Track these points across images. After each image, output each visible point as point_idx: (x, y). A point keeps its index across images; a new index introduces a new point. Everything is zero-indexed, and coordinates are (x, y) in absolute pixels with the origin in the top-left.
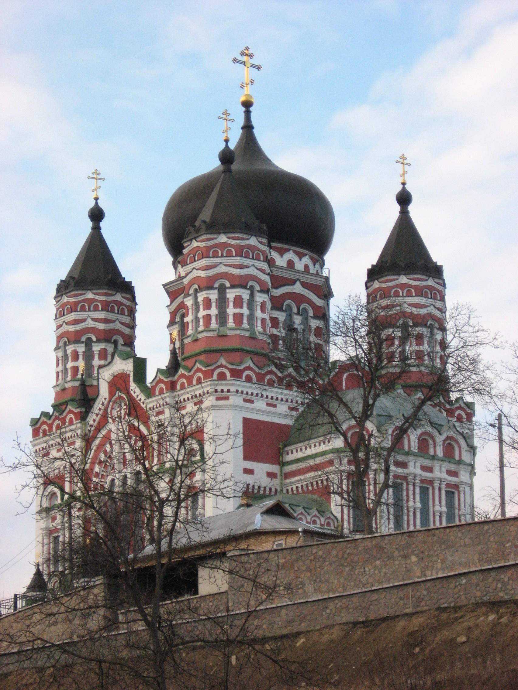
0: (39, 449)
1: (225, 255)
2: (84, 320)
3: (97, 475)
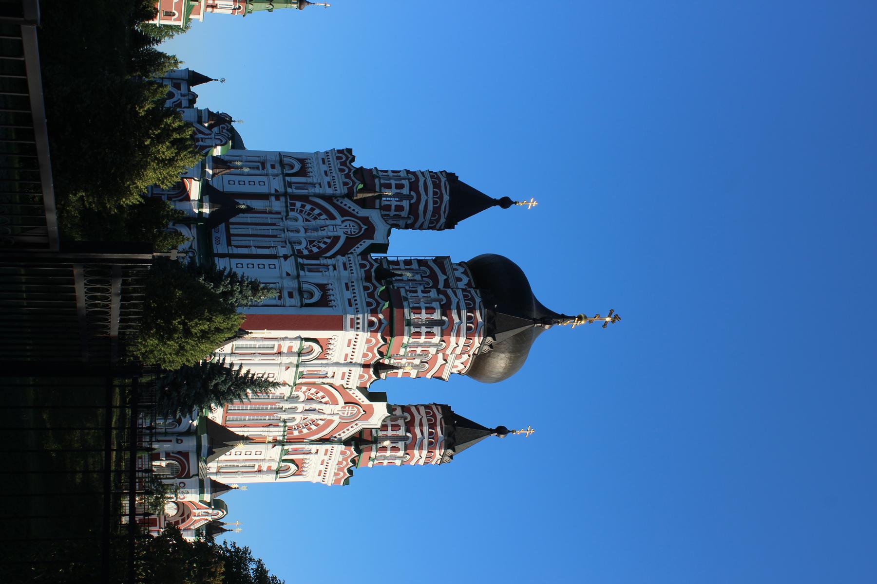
0: (329, 156)
1: (468, 325)
3: (303, 206)
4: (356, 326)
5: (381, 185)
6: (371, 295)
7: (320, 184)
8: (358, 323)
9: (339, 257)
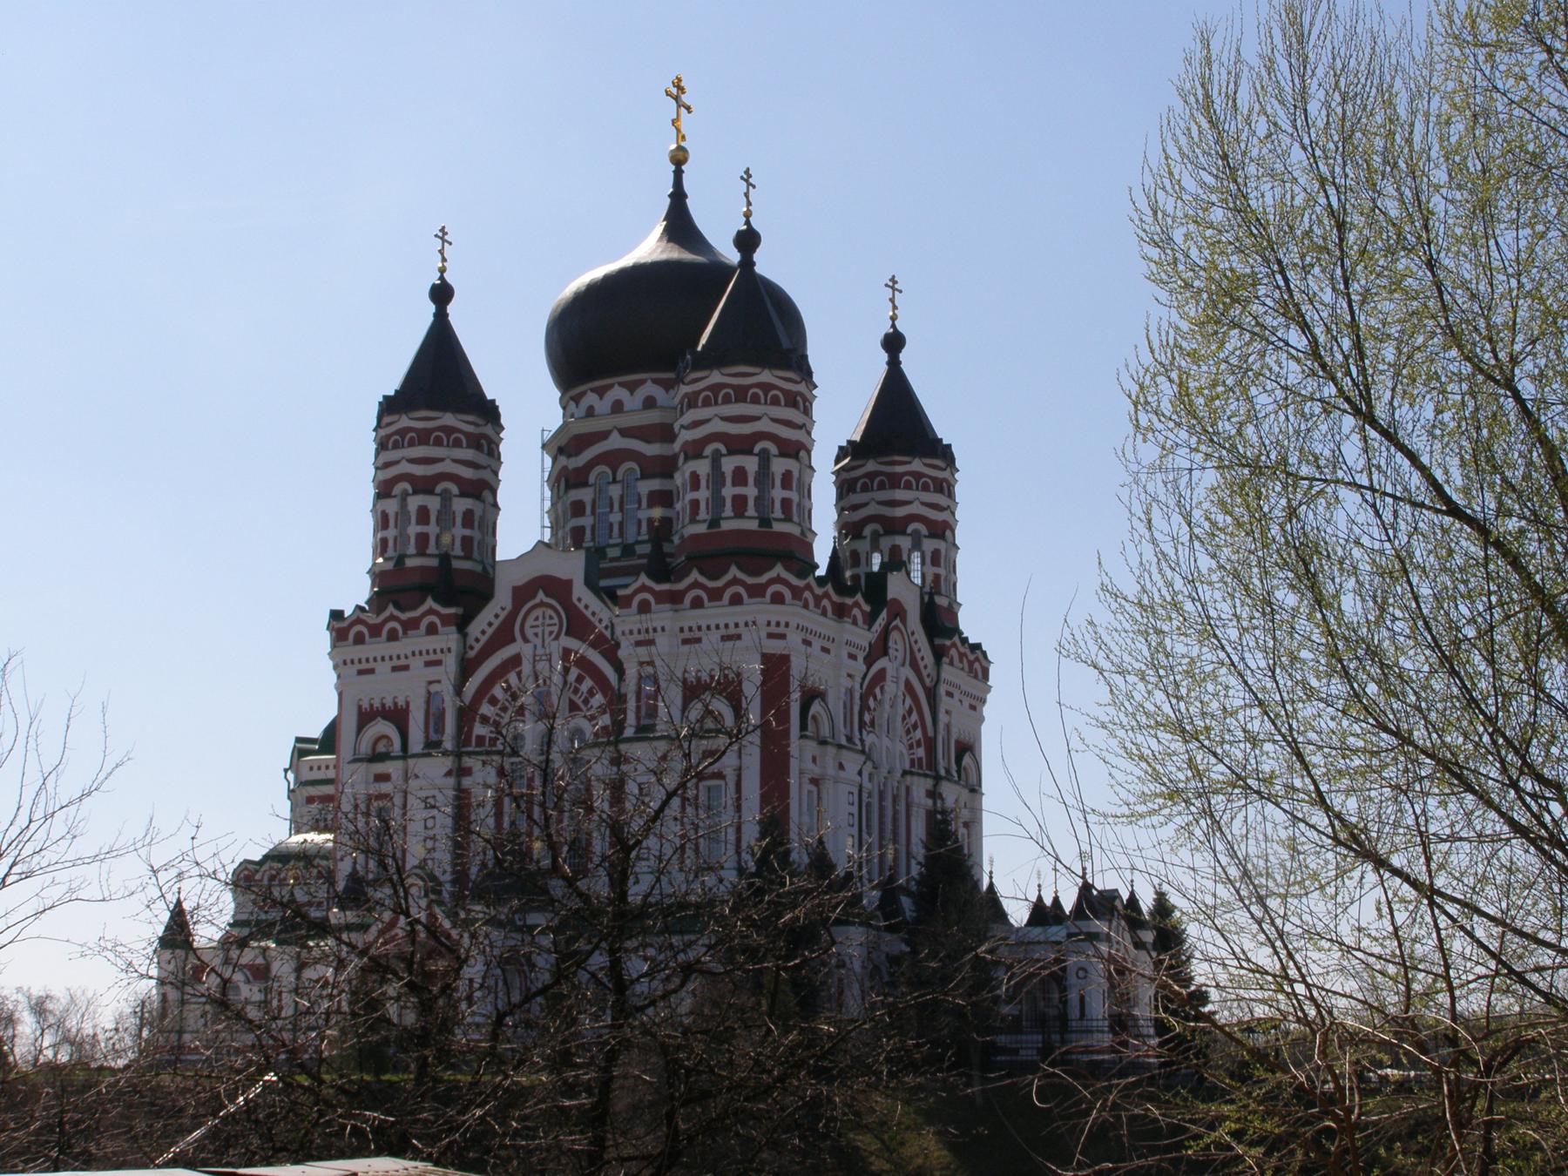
3: (485, 720)
4: (781, 630)
5: (421, 552)
6: (716, 595)
7: (430, 683)
8: (778, 624)
9: (622, 654)
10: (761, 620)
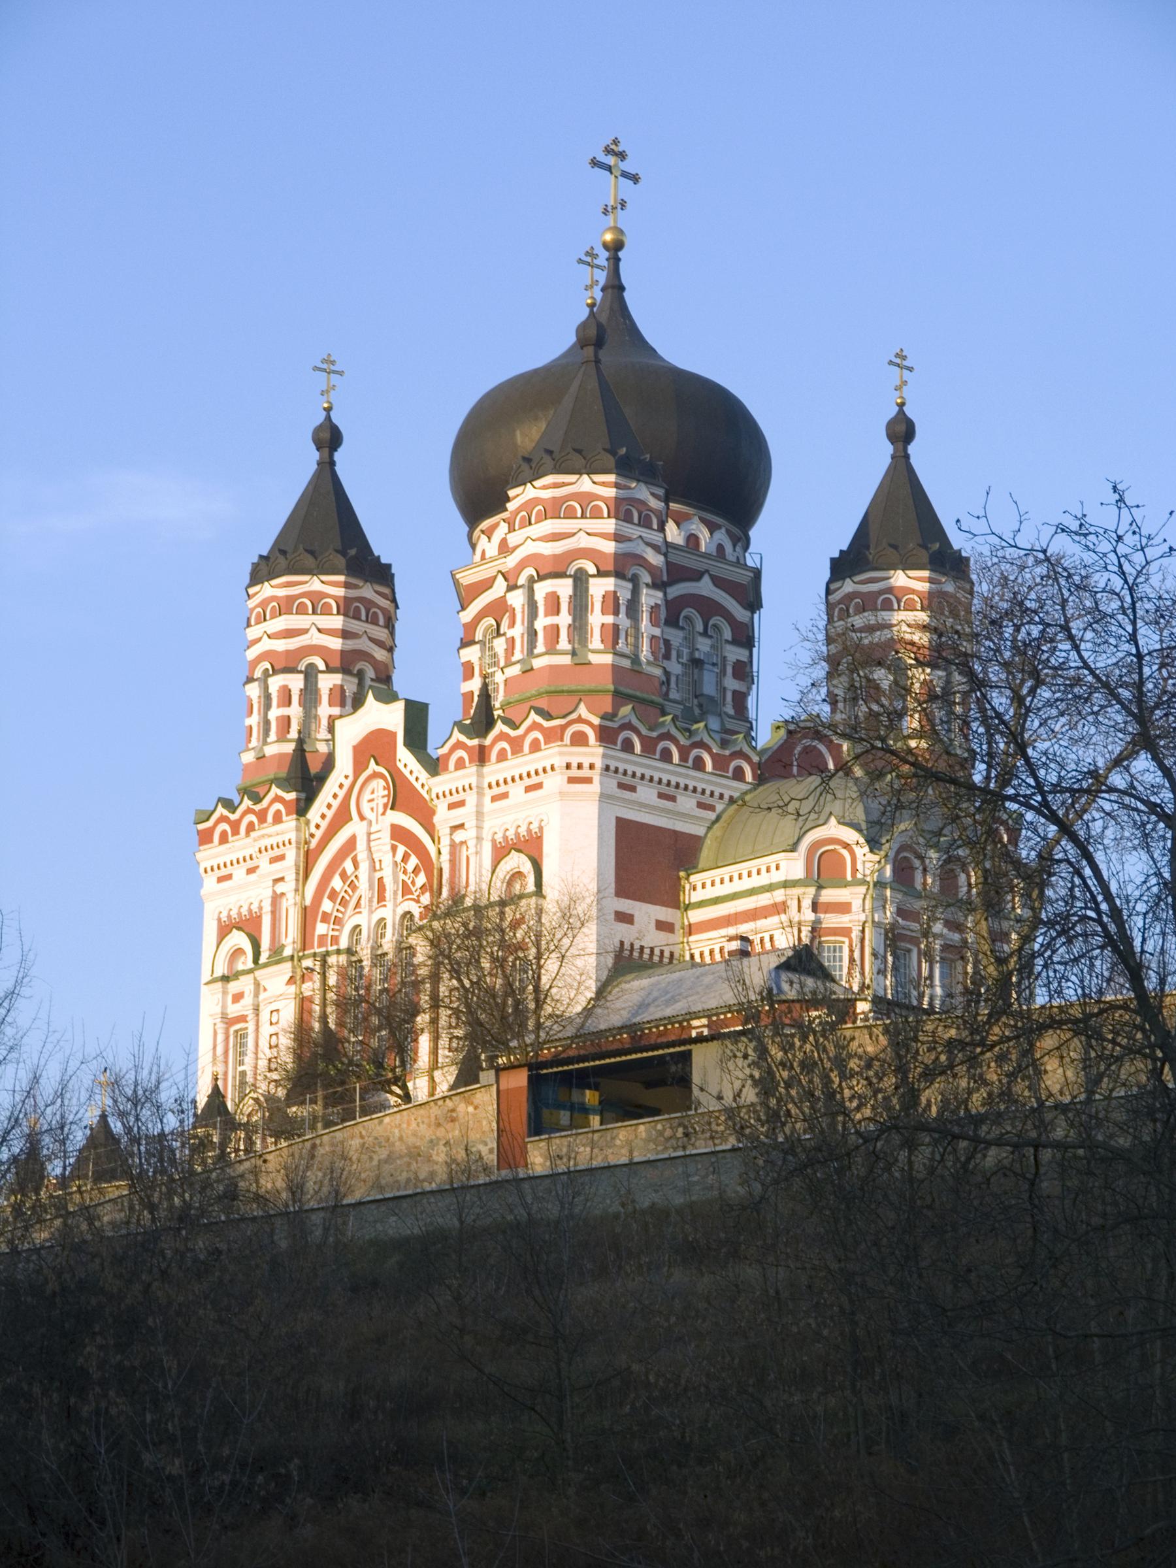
2: (305, 631)
3: (326, 918)
4: (585, 773)
5: (282, 738)
7: (276, 881)
8: (580, 766)
9: (436, 819)
10: (559, 762)
